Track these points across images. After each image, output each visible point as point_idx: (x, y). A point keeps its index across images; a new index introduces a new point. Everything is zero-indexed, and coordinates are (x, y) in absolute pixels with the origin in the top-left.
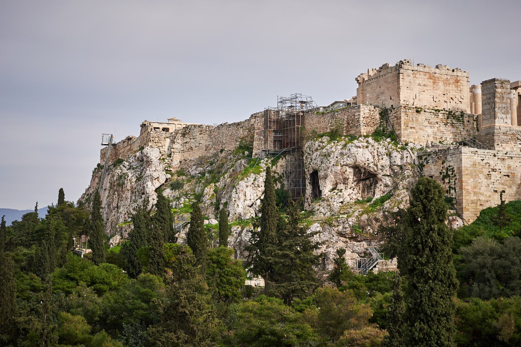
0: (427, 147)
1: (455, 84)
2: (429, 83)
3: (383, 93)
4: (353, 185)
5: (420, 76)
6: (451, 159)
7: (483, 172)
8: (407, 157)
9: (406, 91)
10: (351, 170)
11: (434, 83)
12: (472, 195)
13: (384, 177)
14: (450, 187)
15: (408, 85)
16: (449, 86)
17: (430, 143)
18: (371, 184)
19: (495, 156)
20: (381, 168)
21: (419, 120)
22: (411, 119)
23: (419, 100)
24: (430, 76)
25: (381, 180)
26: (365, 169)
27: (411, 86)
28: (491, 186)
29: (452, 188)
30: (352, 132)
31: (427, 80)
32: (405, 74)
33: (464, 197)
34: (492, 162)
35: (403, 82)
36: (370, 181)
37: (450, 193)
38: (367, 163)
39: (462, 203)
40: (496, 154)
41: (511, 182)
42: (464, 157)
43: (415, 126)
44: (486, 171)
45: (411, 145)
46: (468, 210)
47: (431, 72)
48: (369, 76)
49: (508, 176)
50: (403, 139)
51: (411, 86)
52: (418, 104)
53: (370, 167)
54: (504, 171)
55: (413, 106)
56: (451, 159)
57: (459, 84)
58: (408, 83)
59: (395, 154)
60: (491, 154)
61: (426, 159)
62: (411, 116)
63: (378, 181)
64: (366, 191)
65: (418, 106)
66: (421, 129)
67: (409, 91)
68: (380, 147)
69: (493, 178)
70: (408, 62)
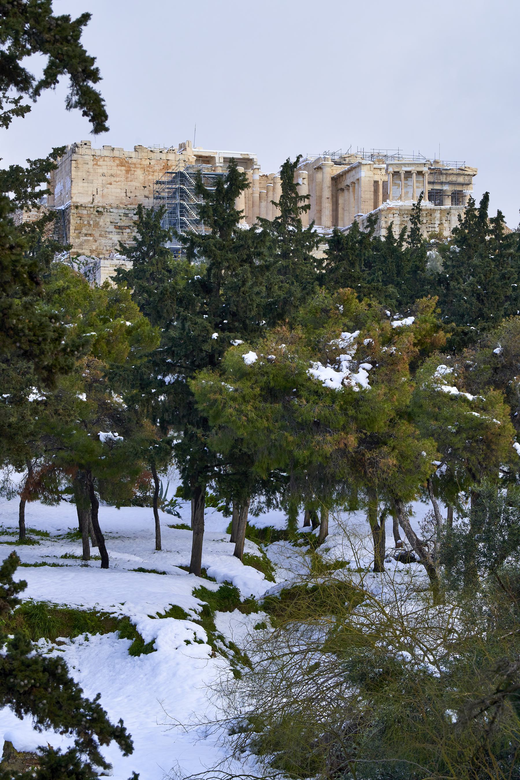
2: (119, 172)
5: (105, 163)
9: (81, 184)
11: (127, 171)
15: (85, 176)
16: (153, 175)
21: (100, 224)
22: (86, 223)
23: (103, 196)
24: (121, 163)
31: (115, 168)
32: (80, 161)
35: (77, 171)
51: (90, 178)
52: (99, 201)
58: (84, 173)
62: (87, 219)
65: (100, 204)
67: (86, 184)
70: (85, 144)
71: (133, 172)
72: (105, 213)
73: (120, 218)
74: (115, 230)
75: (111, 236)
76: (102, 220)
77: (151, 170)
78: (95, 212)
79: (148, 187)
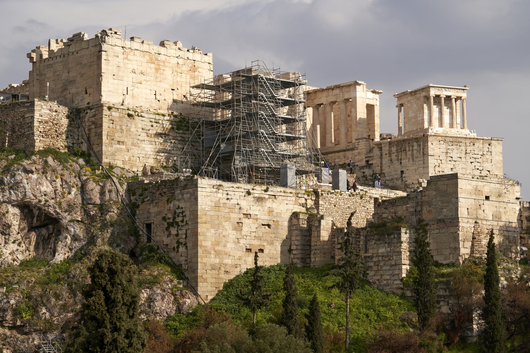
0: (145, 174)
1: (191, 73)
2: (149, 70)
3: (72, 82)
4: (19, 237)
6: (180, 197)
7: (230, 218)
8: (110, 191)
9: (111, 81)
10: (17, 211)
11: (157, 70)
12: (212, 256)
13: (72, 224)
14: (179, 243)
15: (115, 72)
16: (181, 77)
17: (148, 168)
18: (49, 238)
19: (249, 193)
20: (66, 208)
22: (118, 127)
25: (67, 229)
26: (40, 209)
27: (121, 74)
28: (242, 241)
29: (182, 243)
30: (21, 146)
31: (145, 64)
32: (110, 52)
33: (199, 259)
34: (244, 203)
36: (48, 229)
37: (178, 251)
38: (43, 199)
39: (197, 269)
40: (251, 191)
41: (273, 236)
42: (201, 194)
43: (126, 140)
44: (235, 216)
45: (117, 171)
46: (205, 280)
47: (153, 52)
48: (51, 52)
49: (269, 226)
50: (105, 160)
51: (121, 74)
52: (130, 103)
53: (49, 206)
54: (263, 217)
55: (122, 107)
56: (180, 197)
57: (196, 73)
59: (91, 185)
60: (243, 190)
61: (140, 195)
63: (62, 229)
64: (41, 247)
65: (130, 107)
66: (133, 144)
67: (116, 81)
68: (66, 173)
69: (245, 229)
70: (116, 33)
71: (162, 71)
72: (136, 117)
73: (150, 124)
74: (147, 138)
75: (143, 146)
76: (133, 126)
77: (179, 71)
78: (126, 116)
79: (176, 90)
